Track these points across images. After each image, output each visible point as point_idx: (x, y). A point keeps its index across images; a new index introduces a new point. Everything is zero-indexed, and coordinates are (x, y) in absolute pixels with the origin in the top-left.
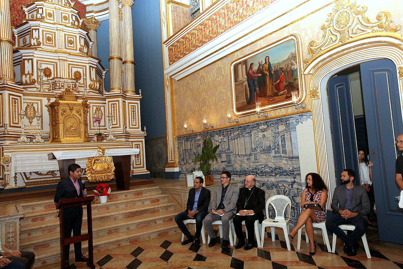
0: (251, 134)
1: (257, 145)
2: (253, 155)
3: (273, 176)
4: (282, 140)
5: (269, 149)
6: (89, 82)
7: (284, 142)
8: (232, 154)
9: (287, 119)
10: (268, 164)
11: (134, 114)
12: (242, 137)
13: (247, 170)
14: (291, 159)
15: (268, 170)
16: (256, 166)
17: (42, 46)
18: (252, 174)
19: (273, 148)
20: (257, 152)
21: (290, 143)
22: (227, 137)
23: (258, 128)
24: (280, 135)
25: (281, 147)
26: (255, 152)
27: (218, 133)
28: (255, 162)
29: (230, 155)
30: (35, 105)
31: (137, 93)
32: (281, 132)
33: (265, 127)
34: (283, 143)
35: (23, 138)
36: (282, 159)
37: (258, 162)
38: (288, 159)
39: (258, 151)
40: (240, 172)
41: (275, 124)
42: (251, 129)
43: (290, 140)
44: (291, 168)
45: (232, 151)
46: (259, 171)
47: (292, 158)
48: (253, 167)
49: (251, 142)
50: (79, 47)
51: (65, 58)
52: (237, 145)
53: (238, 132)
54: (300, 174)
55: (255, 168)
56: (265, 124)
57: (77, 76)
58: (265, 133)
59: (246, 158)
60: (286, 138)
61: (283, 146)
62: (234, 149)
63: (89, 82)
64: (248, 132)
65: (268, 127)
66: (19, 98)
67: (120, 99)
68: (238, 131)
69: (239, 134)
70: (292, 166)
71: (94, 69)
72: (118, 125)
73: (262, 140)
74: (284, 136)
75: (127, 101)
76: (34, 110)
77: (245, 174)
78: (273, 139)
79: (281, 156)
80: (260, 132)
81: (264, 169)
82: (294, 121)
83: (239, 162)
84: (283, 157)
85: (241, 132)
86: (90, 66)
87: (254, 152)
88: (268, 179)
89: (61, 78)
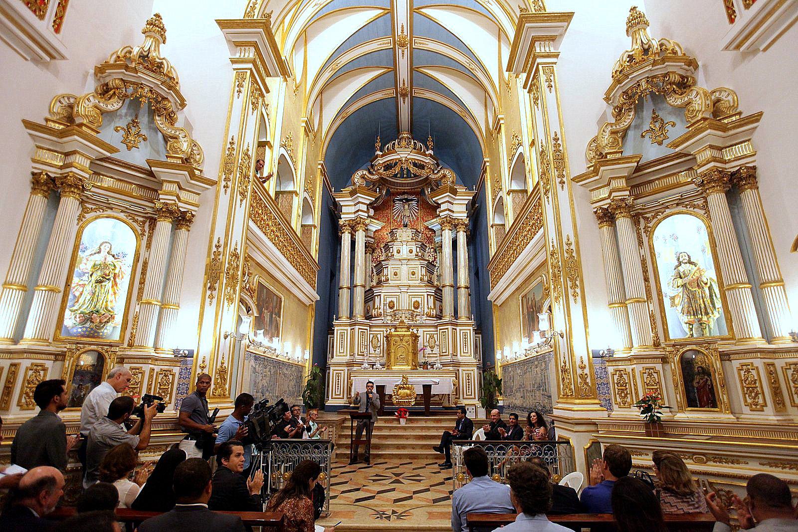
6: (426, 310)
11: (465, 341)
17: (390, 282)
30: (379, 336)
31: (470, 319)
35: (366, 365)
50: (420, 276)
51: (406, 291)
57: (417, 305)
63: (426, 310)
66: (366, 331)
67: (450, 327)
71: (432, 297)
72: (447, 353)
75: (458, 328)
76: (378, 340)
86: (428, 295)
89: (399, 310)
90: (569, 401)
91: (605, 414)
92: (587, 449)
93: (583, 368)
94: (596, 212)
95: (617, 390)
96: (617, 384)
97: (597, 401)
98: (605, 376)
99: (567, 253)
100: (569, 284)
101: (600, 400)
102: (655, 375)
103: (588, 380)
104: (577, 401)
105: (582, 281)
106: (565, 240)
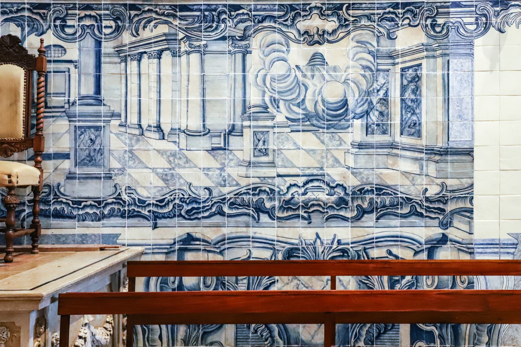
0: (248, 46)
1: (277, 96)
2: (248, 134)
3: (345, 219)
4: (405, 82)
5: (340, 115)
7: (414, 92)
8: (115, 122)
9: (437, 8)
10: (327, 171)
12: (188, 53)
13: (204, 195)
14: (437, 158)
15: (323, 196)
16: (258, 180)
18: (234, 211)
19: (359, 111)
20: (269, 123)
21: (440, 98)
22: (89, 42)
23: (289, 23)
24: (401, 66)
25: (396, 109)
26: (261, 123)
27: (26, 14)
28: (256, 165)
29: (98, 129)
32: (403, 55)
33: (331, 25)
34: (408, 95)
36: (397, 155)
37: (272, 164)
38: (423, 155)
39: (280, 118)
40: (161, 203)
41: (381, 19)
42: (248, 23)
43: (440, 89)
44: (433, 191)
45: (116, 108)
46: (271, 199)
47: (445, 152)
48: (244, 182)
49: (240, 79)
52: (154, 85)
53: (163, 29)
54: (471, 211)
55: (254, 189)
56: (330, 12)
58: (324, 49)
59: (205, 143)
60: (424, 80)
61: (405, 106)
62: (133, 100)
64: (232, 38)
65: (341, 26)
68: (166, 22)
69: (169, 38)
70: (439, 181)
73: (305, 76)
74: (416, 70)
77: (188, 212)
78: (364, 76)
79: (392, 146)
80: (298, 42)
81: (304, 194)
82: (466, 20)
83: (161, 163)
84: (404, 149)
85: (186, 30)
87: (253, 123)
88: (319, 230)
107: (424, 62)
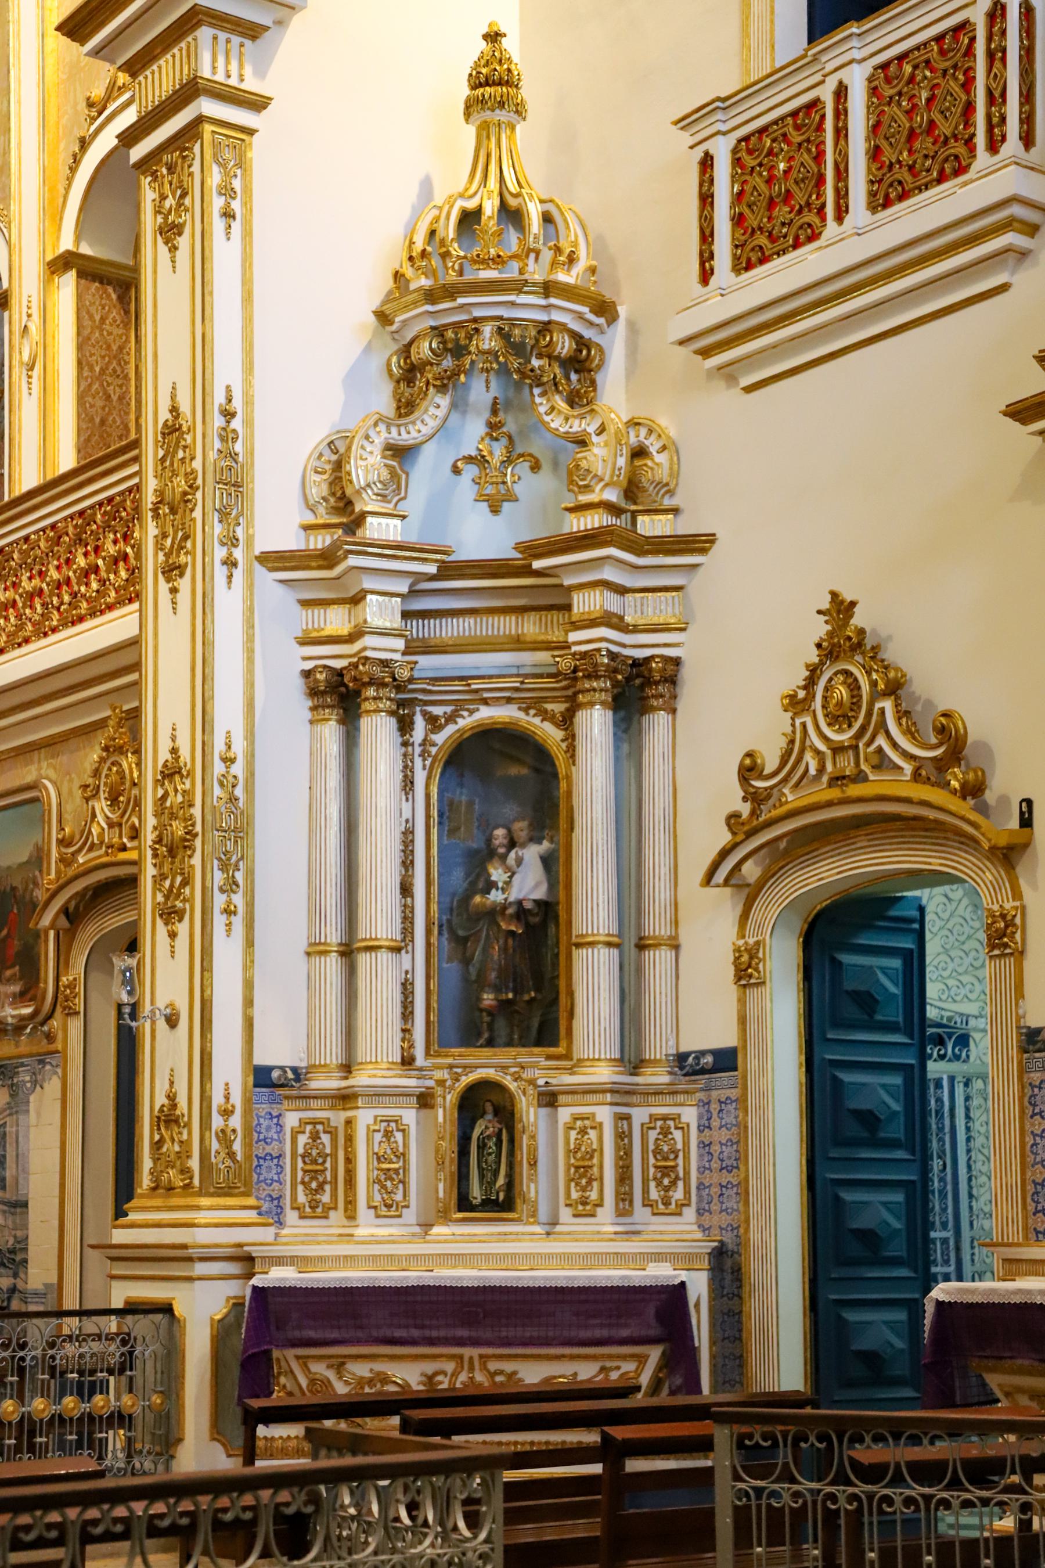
90: (175, 1201)
91: (267, 1234)
92: (219, 1321)
93: (227, 1113)
94: (307, 674)
95: (300, 1174)
96: (303, 1157)
97: (251, 1201)
98: (275, 1137)
99: (221, 784)
100: (219, 877)
101: (258, 1198)
102: (399, 1136)
103: (237, 1147)
104: (205, 1201)
105: (250, 874)
106: (219, 746)
107: (8, 1119)
